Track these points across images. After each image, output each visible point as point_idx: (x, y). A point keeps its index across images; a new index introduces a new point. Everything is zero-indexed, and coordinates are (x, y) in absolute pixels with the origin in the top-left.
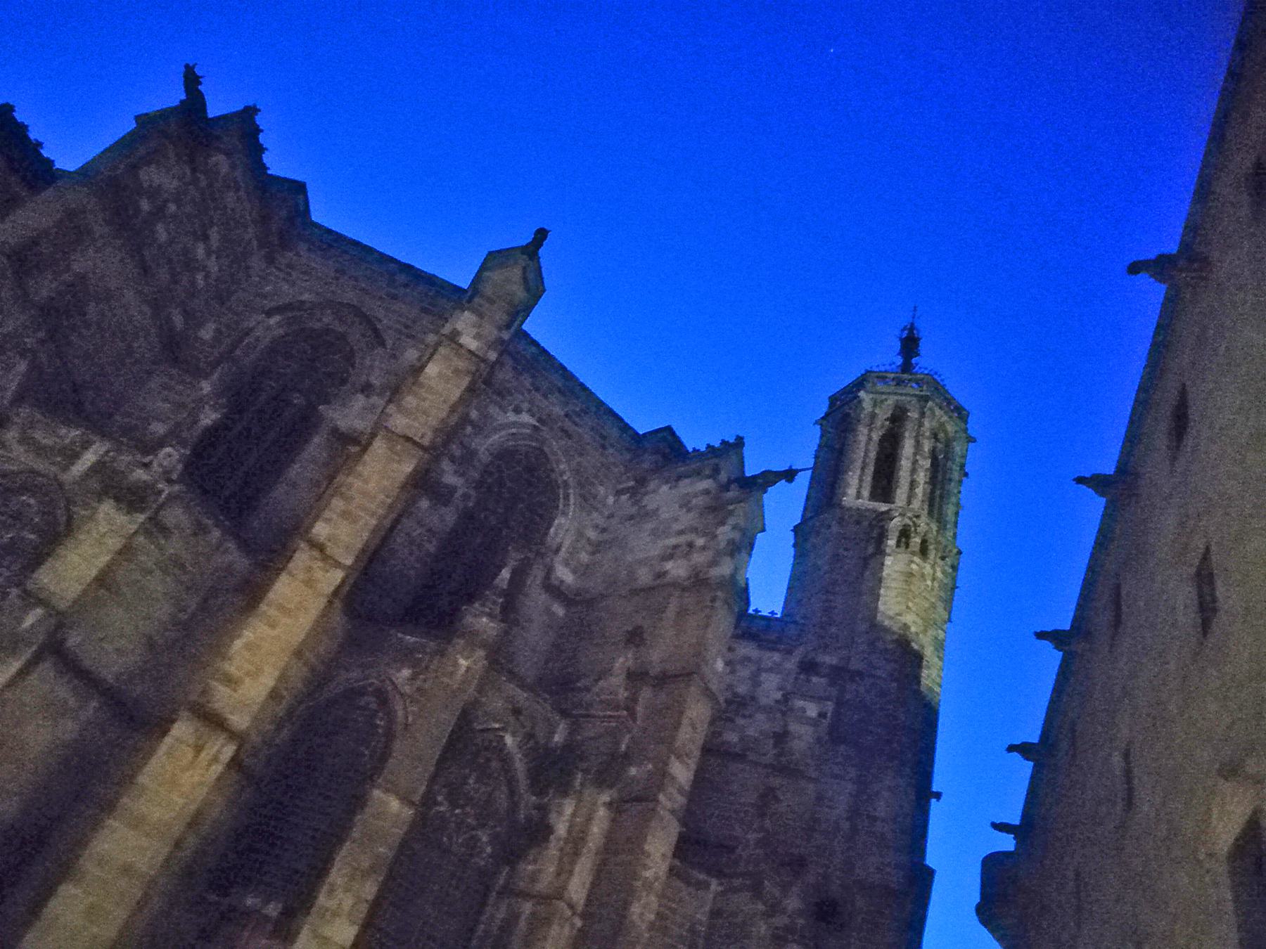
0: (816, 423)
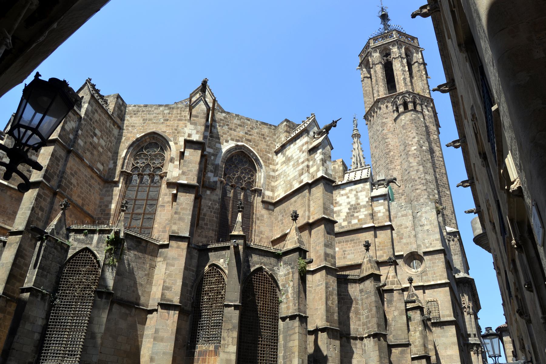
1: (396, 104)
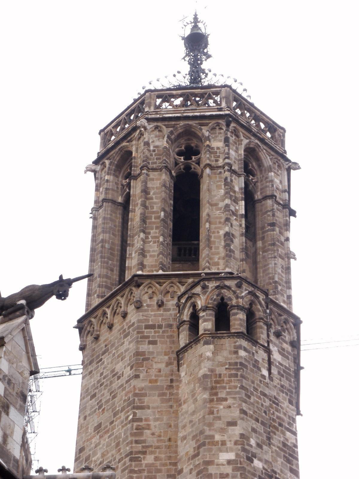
0: (88, 169)
1: (194, 306)
